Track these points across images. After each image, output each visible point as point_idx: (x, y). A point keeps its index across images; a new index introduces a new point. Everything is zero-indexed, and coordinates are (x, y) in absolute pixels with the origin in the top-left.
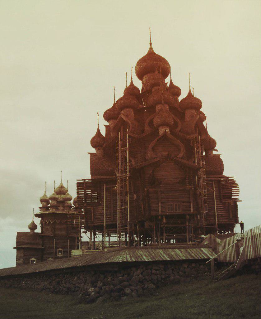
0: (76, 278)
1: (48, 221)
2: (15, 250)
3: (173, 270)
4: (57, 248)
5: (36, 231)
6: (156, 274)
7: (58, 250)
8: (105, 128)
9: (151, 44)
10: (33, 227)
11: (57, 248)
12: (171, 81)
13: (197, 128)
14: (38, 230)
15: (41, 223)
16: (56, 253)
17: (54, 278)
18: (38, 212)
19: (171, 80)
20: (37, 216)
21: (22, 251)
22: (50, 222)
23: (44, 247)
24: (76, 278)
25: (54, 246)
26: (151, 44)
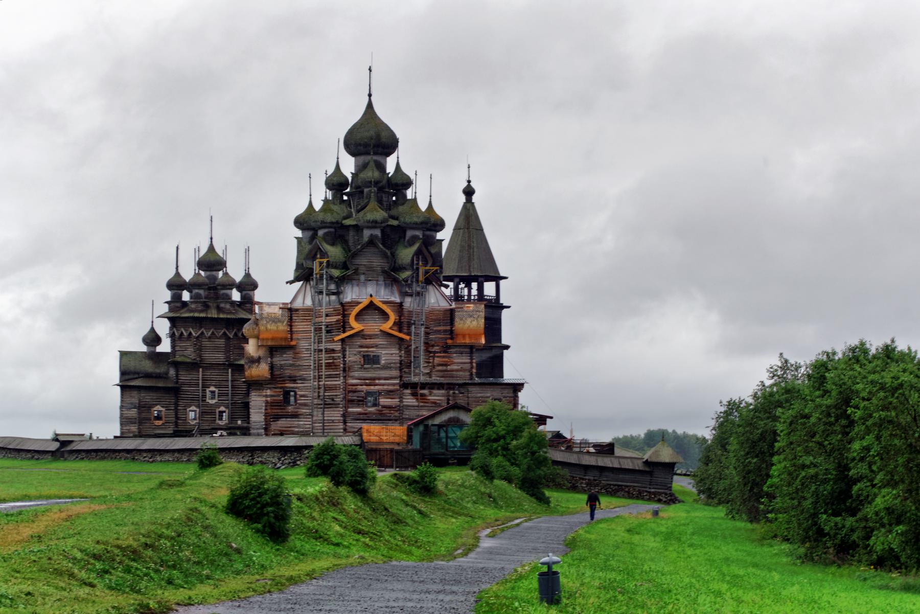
1: (186, 330)
2: (119, 388)
4: (205, 386)
5: (159, 349)
7: (208, 390)
8: (296, 241)
9: (370, 95)
10: (153, 339)
12: (398, 164)
13: (420, 257)
14: (165, 347)
16: (204, 396)
19: (398, 160)
25: (200, 381)
26: (370, 95)
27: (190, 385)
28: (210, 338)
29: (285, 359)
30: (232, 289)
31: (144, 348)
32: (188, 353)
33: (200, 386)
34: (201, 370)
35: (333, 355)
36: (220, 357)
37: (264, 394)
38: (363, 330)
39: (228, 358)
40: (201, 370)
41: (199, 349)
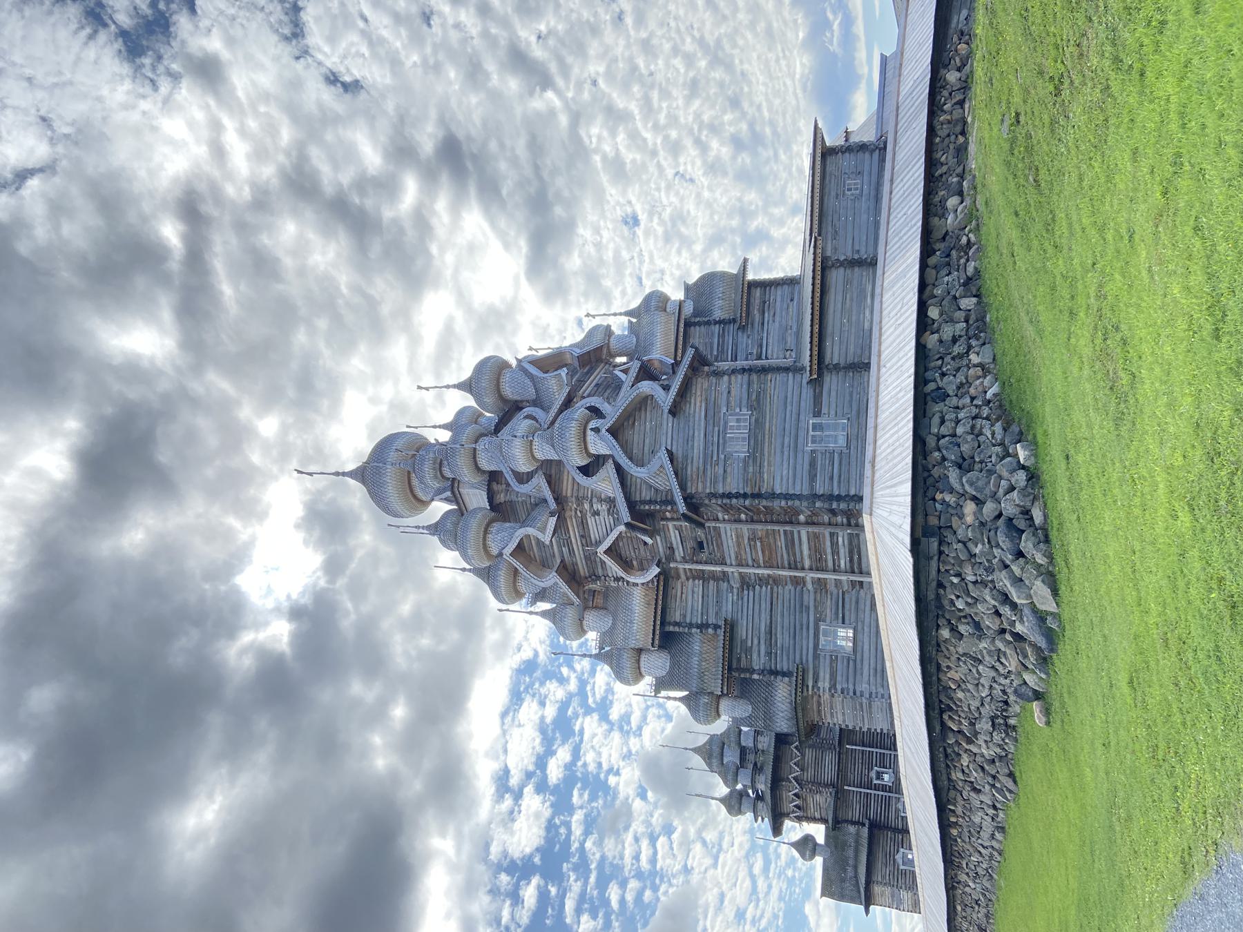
0: (960, 695)
1: (793, 801)
3: (943, 375)
4: (870, 786)
5: (821, 839)
6: (958, 422)
10: (806, 846)
11: (870, 786)
14: (818, 832)
15: (799, 819)
17: (960, 775)
18: (765, 824)
20: (777, 830)
21: (877, 889)
22: (795, 795)
23: (867, 822)
24: (960, 695)
27: (868, 806)
28: (802, 770)
29: (756, 642)
30: (741, 730)
31: (819, 861)
32: (822, 800)
33: (869, 791)
34: (846, 788)
35: (746, 541)
36: (830, 759)
37: (827, 696)
38: (670, 454)
39: (831, 748)
40: (846, 788)
41: (818, 784)
